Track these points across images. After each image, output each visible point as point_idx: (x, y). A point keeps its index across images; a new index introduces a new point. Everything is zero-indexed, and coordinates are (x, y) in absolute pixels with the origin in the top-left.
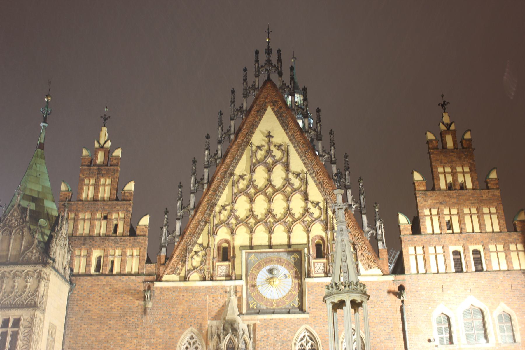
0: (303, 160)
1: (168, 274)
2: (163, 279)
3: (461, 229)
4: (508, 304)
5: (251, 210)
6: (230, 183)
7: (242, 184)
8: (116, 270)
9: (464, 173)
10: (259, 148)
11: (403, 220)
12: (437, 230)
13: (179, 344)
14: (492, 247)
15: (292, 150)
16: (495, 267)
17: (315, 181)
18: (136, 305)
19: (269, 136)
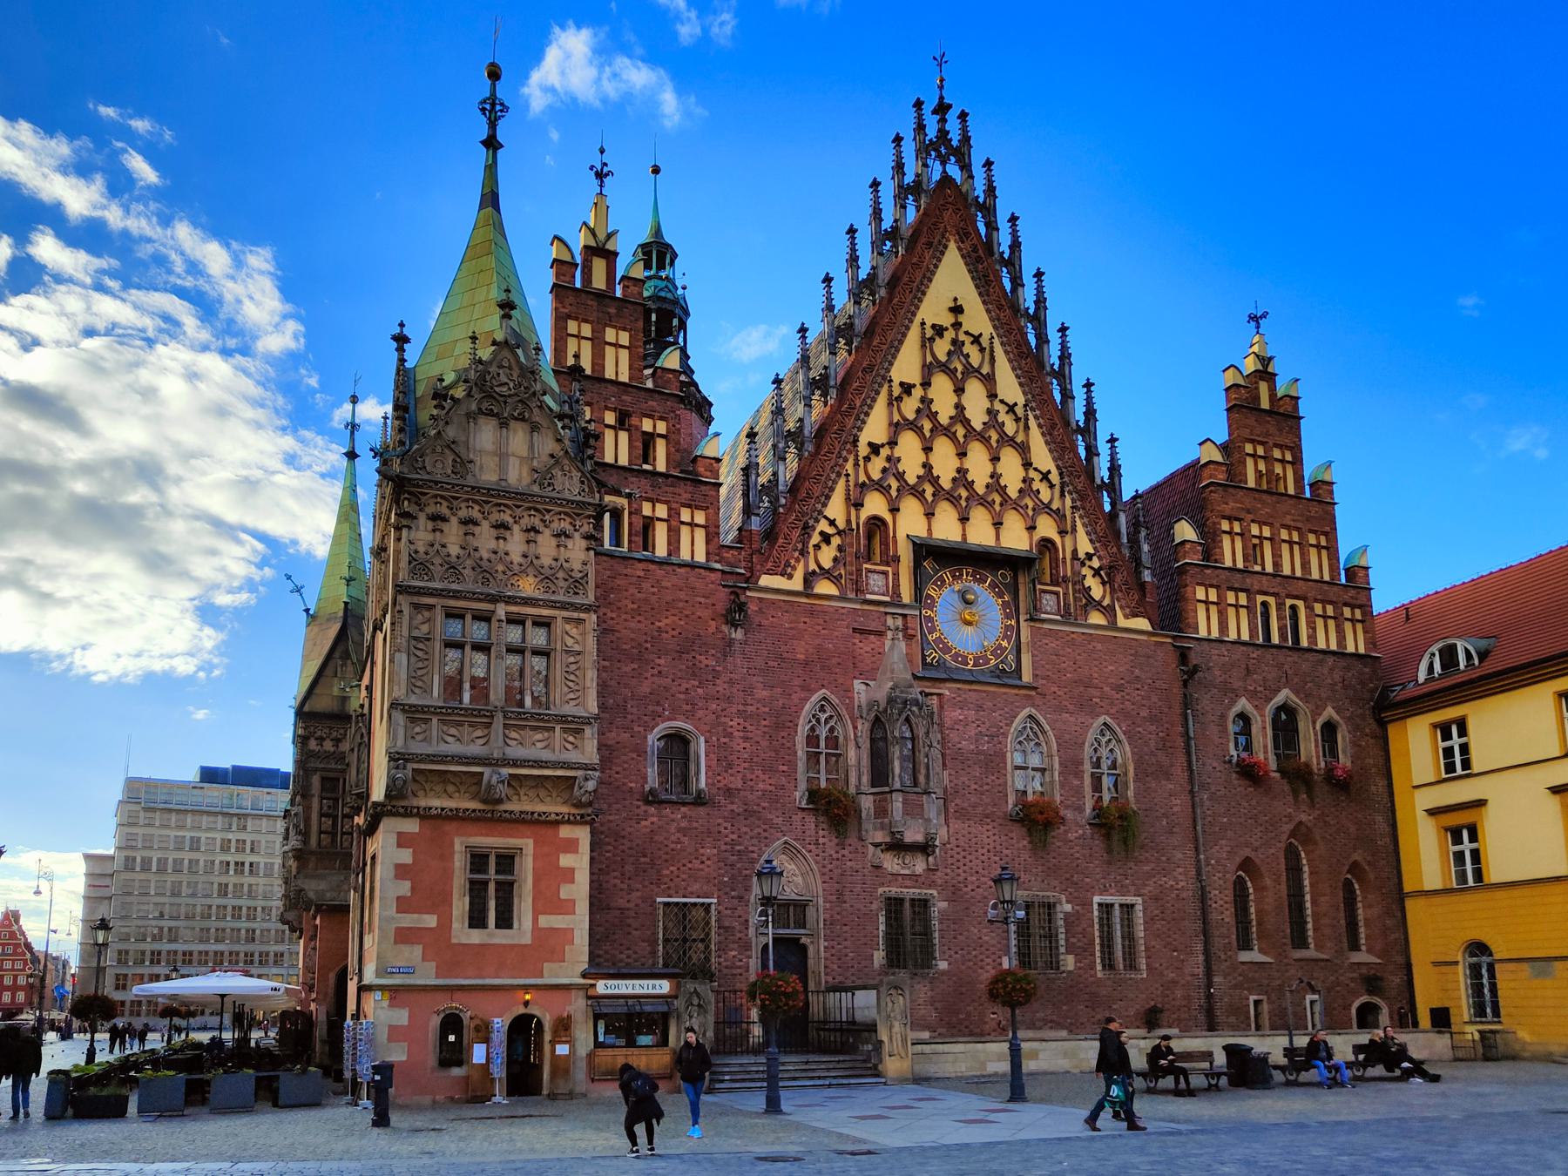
0: (1017, 377)
3: (1277, 564)
4: (1338, 710)
5: (927, 466)
6: (882, 400)
7: (910, 407)
8: (661, 550)
9: (1282, 461)
11: (1185, 531)
12: (1240, 565)
13: (801, 721)
14: (1318, 608)
16: (1321, 645)
17: (1040, 426)
18: (711, 630)
19: (957, 310)
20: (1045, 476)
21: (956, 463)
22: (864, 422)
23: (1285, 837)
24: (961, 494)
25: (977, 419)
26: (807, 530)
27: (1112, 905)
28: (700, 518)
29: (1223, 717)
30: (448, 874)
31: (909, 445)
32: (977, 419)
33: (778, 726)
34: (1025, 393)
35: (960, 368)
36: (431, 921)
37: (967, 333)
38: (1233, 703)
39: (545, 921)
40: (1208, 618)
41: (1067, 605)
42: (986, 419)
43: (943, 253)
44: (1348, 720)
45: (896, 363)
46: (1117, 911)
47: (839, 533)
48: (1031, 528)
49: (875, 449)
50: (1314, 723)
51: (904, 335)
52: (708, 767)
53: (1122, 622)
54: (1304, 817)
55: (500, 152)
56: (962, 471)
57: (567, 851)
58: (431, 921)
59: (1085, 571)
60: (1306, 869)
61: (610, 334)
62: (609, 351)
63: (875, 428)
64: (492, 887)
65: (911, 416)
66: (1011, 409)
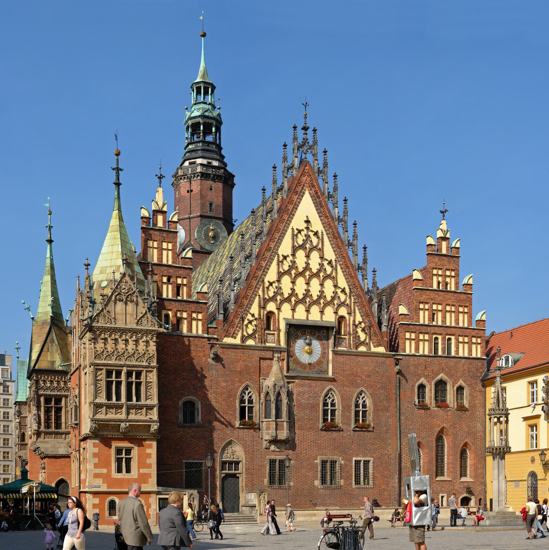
0: (333, 248)
1: (227, 336)
2: (224, 341)
5: (293, 290)
10: (300, 231)
15: (326, 237)
19: (308, 222)
20: (343, 291)
21: (305, 287)
22: (267, 273)
23: (436, 434)
24: (307, 300)
25: (315, 267)
26: (243, 319)
27: (360, 461)
28: (200, 316)
29: (413, 386)
30: (109, 456)
31: (286, 281)
32: (315, 267)
33: (229, 397)
34: (336, 255)
35: (308, 246)
36: (105, 471)
37: (312, 231)
38: (418, 380)
39: (142, 471)
40: (410, 346)
41: (350, 343)
42: (318, 267)
43: (302, 196)
44: (469, 385)
45: (281, 247)
46: (362, 464)
47: (256, 319)
48: (336, 313)
49: (271, 284)
50: (453, 387)
51: (285, 234)
52: (202, 413)
53: (374, 349)
54: (445, 425)
55: (120, 186)
56: (308, 291)
57: (148, 448)
58: (105, 471)
59: (359, 330)
60: (446, 445)
61: (165, 245)
62: (165, 252)
63: (271, 275)
64: (124, 460)
65: (286, 268)
66: (330, 263)
